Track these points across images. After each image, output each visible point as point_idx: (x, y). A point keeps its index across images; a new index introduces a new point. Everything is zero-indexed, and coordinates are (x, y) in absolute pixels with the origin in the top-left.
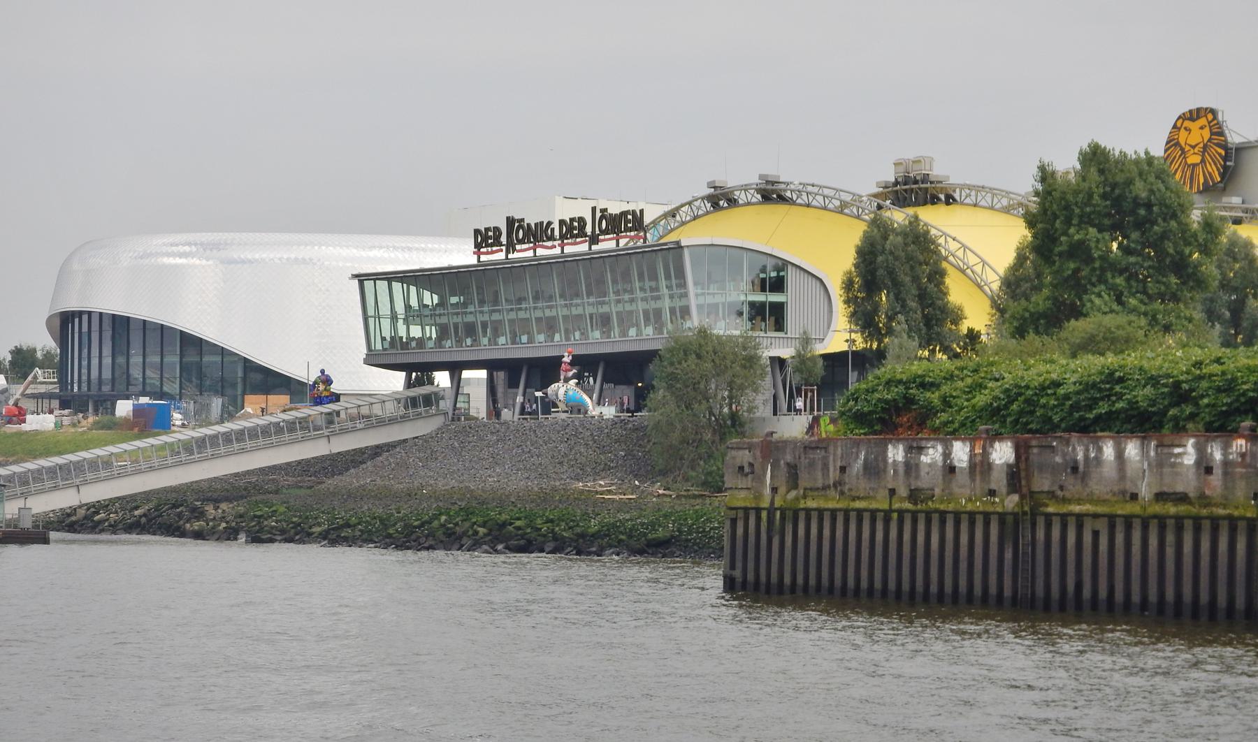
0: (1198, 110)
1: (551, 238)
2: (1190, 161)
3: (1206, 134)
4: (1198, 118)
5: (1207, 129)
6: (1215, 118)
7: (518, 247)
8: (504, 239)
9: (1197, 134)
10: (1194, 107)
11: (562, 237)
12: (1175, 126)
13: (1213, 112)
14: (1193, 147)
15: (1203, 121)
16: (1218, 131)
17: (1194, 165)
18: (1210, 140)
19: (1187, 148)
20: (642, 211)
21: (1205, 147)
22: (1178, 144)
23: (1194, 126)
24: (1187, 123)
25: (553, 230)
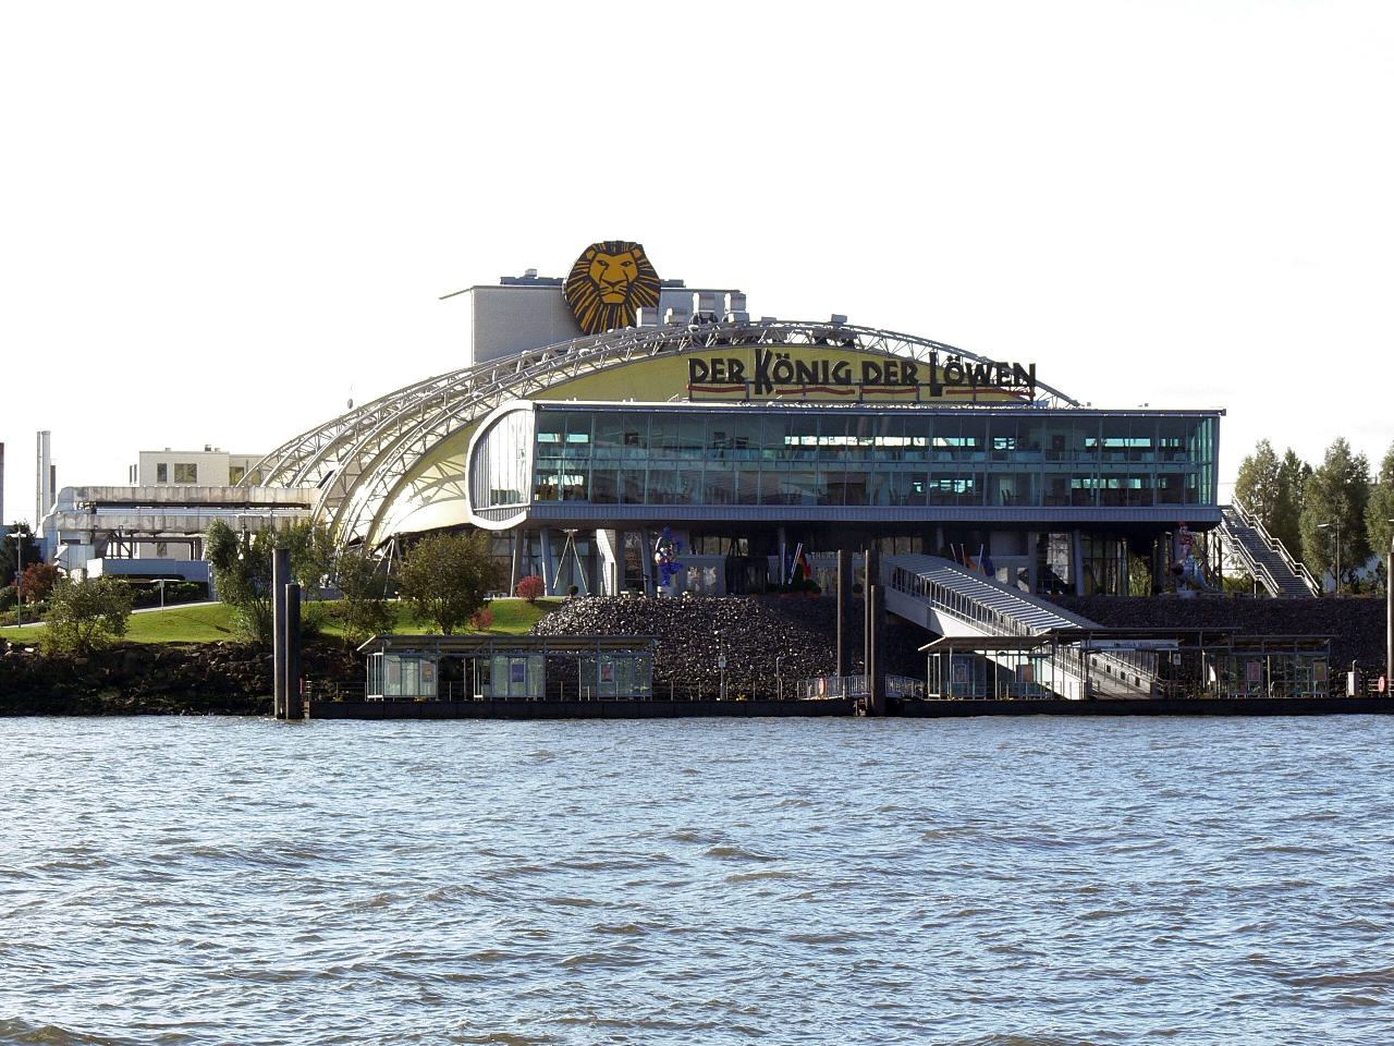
0: (619, 244)
1: (847, 381)
2: (607, 299)
3: (632, 272)
4: (619, 252)
5: (634, 265)
6: (644, 256)
7: (776, 387)
8: (749, 373)
9: (616, 271)
10: (613, 238)
11: (867, 381)
12: (583, 257)
13: (640, 247)
14: (613, 285)
15: (627, 257)
16: (645, 270)
17: (614, 306)
18: (637, 279)
19: (603, 285)
20: (1032, 367)
21: (630, 286)
22: (589, 278)
23: (615, 261)
24: (601, 256)
25: (848, 372)
